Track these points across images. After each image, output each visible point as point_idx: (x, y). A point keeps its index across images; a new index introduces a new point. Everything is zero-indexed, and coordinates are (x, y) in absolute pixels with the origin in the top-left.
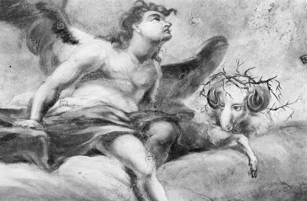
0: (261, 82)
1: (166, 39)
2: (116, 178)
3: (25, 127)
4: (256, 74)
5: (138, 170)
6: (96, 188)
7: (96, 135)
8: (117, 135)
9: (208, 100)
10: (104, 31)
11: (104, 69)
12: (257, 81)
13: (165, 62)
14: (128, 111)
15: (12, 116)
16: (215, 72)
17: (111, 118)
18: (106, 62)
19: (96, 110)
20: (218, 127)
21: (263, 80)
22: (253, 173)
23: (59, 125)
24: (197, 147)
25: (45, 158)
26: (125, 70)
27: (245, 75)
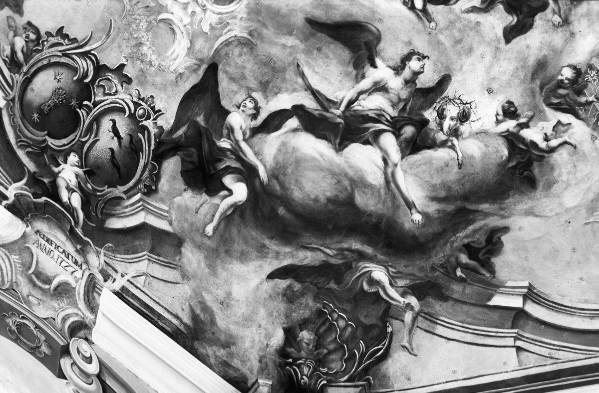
0: (467, 103)
1: (422, 72)
2: (376, 165)
3: (335, 114)
4: (465, 99)
5: (390, 159)
6: (361, 170)
7: (371, 130)
8: (383, 131)
9: (438, 113)
10: (392, 64)
11: (386, 86)
12: (465, 103)
13: (419, 86)
14: (392, 115)
15: (331, 105)
16: (444, 96)
17: (383, 119)
18: (388, 82)
19: (375, 112)
20: (441, 132)
21: (468, 102)
22: (460, 166)
24: (428, 146)
25: (338, 141)
27: (459, 99)
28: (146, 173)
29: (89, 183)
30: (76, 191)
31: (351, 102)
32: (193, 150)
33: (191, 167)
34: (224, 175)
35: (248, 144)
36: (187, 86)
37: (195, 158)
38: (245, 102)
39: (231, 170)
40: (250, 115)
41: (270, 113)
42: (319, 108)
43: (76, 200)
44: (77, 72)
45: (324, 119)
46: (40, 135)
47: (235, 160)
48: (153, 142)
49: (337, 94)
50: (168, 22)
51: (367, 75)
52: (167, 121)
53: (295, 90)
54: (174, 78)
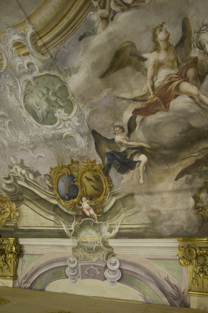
1: (169, 35)
3: (151, 98)
11: (160, 62)
18: (159, 59)
23: (160, 92)
26: (165, 58)
28: (107, 183)
29: (92, 202)
30: (90, 209)
31: (153, 87)
32: (115, 161)
33: (119, 167)
34: (132, 158)
35: (131, 141)
36: (94, 146)
37: (118, 163)
38: (115, 130)
39: (133, 155)
40: (122, 132)
41: (127, 124)
42: (143, 103)
43: (92, 212)
44: (65, 174)
45: (149, 105)
46: (71, 201)
47: (132, 150)
48: (100, 171)
49: (144, 89)
50: (68, 136)
51: (146, 68)
52: (99, 161)
53: (126, 107)
54: (87, 148)
